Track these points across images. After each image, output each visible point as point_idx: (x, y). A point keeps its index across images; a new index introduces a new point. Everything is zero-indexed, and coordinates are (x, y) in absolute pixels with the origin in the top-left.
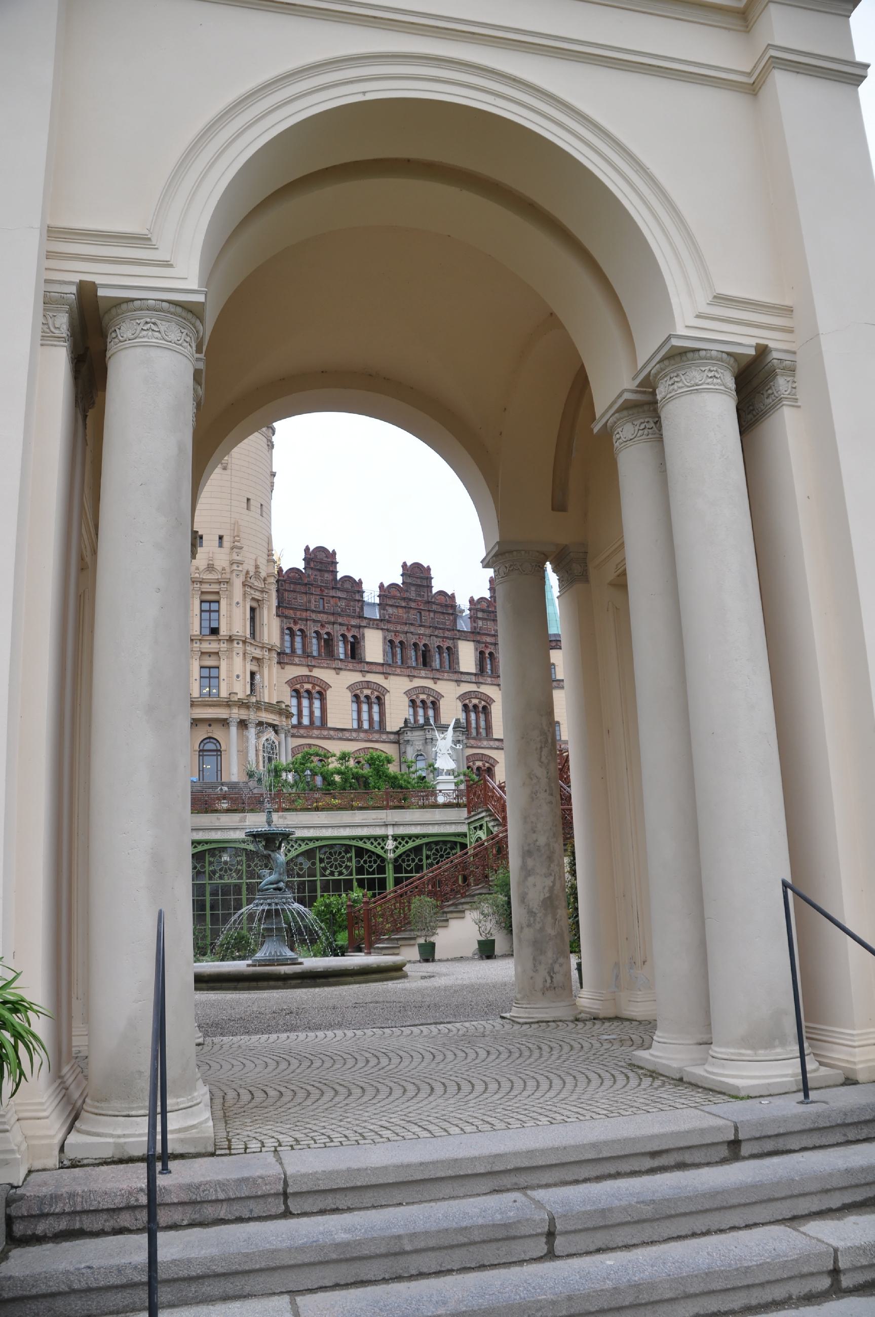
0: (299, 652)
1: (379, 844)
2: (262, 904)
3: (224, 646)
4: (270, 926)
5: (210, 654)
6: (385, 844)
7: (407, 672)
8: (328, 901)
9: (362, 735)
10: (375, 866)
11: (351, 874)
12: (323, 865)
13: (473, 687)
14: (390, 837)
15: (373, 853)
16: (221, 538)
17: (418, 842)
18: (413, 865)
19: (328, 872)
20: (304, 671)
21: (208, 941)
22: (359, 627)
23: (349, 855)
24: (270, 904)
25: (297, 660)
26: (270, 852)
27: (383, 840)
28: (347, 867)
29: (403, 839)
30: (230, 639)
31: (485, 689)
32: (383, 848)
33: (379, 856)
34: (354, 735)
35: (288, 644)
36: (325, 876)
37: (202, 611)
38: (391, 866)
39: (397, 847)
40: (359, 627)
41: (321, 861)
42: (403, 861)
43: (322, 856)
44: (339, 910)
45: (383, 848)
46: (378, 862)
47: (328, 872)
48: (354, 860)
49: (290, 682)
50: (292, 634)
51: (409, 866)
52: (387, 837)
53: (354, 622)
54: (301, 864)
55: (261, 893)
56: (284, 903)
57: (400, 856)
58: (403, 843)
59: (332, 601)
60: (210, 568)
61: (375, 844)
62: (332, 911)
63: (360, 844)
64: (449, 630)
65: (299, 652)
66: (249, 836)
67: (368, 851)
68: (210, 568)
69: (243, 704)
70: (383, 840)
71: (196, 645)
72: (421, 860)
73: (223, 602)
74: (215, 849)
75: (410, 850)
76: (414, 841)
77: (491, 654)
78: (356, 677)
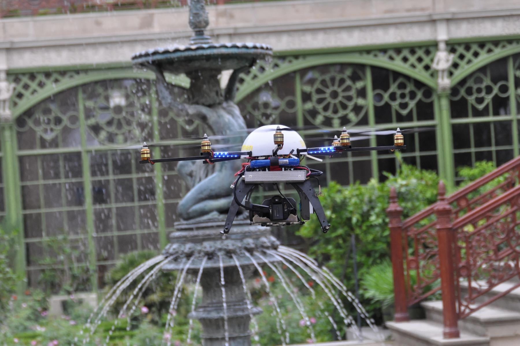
1: (420, 60)
2: (189, 256)
4: (214, 315)
6: (432, 60)
8: (338, 198)
10: (412, 104)
11: (364, 122)
12: (309, 106)
14: (442, 46)
15: (408, 78)
17: (498, 53)
18: (488, 99)
19: (320, 119)
21: (92, 265)
23: (359, 85)
24: (210, 256)
26: (205, 110)
27: (428, 53)
28: (357, 109)
29: (468, 48)
32: (427, 68)
33: (419, 84)
36: (315, 127)
38: (445, 103)
39: (455, 65)
41: (306, 97)
42: (469, 91)
43: (308, 89)
44: (365, 216)
45: (427, 68)
46: (419, 95)
47: (320, 119)
48: (370, 93)
51: (480, 101)
52: (435, 45)
54: (266, 105)
55: (183, 224)
56: (250, 251)
57: (463, 82)
58: (469, 55)
61: (413, 59)
62: (350, 219)
63: (382, 61)
66: (142, 65)
67: (397, 75)
70: (428, 53)
72: (504, 89)
74: (96, 83)
75: (483, 70)
76: (490, 51)
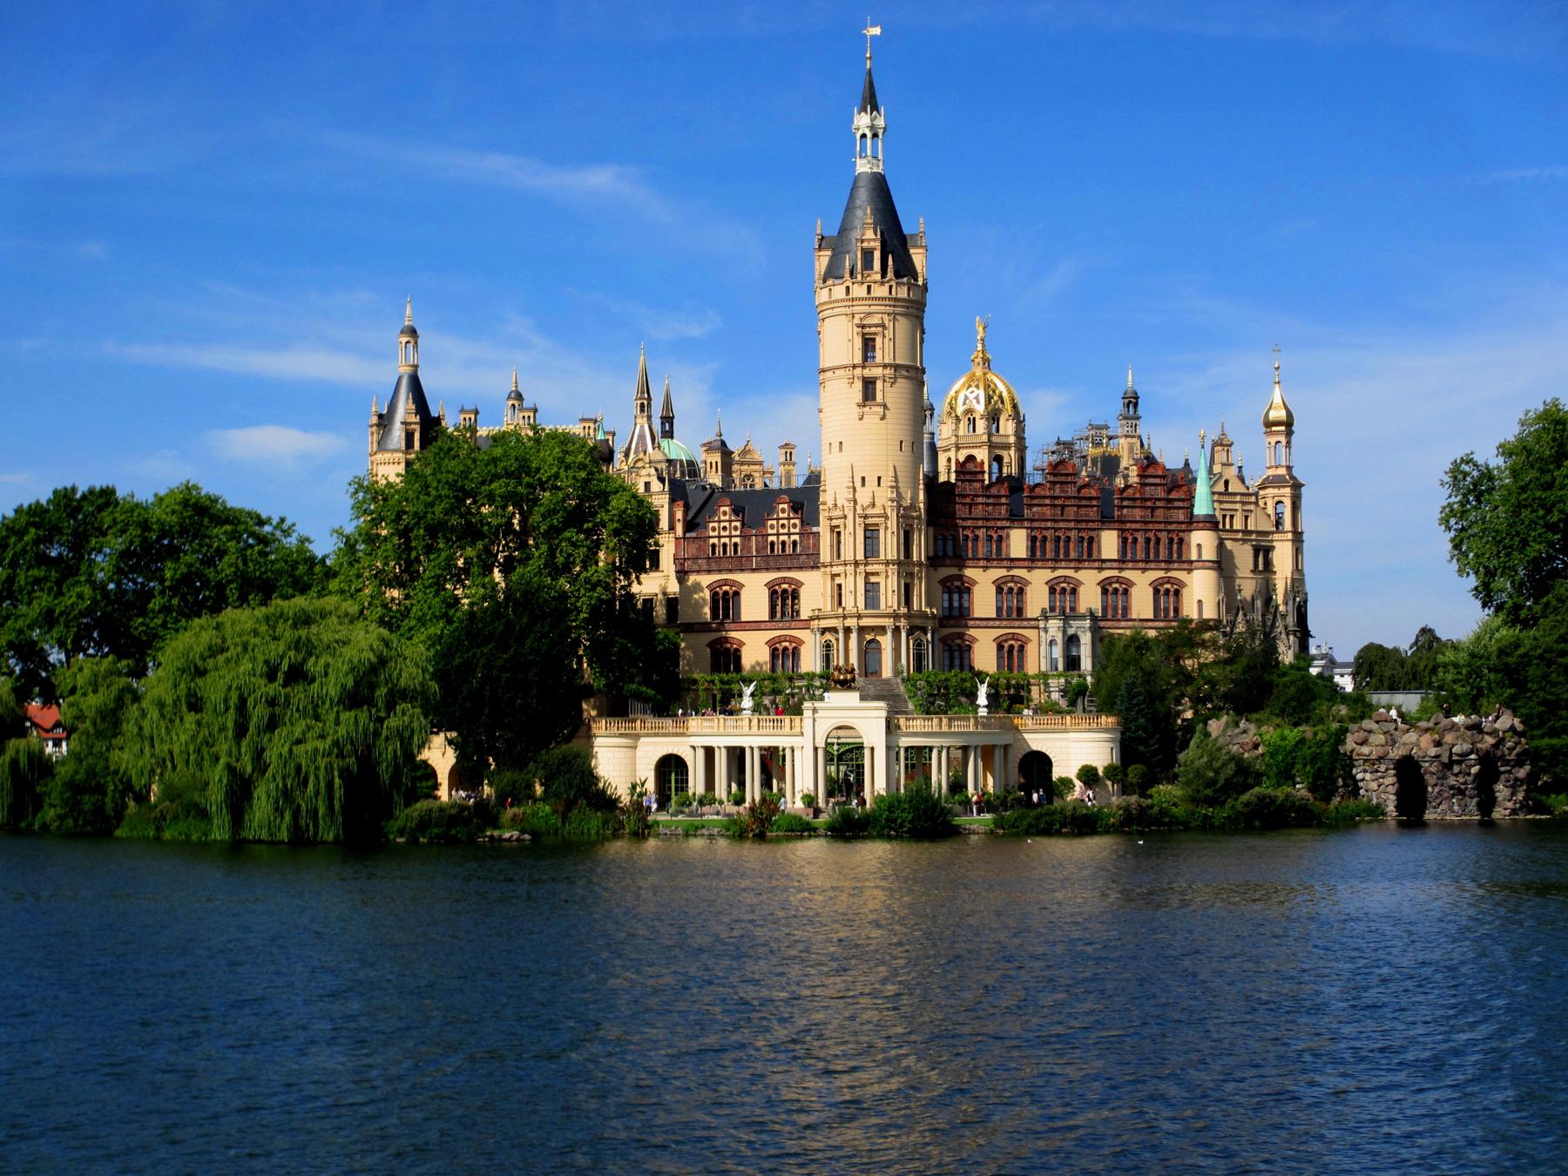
0: (950, 553)
3: (881, 568)
5: (873, 574)
7: (1050, 564)
9: (1004, 623)
13: (1115, 573)
16: (879, 478)
20: (954, 571)
22: (1002, 528)
25: (948, 562)
30: (887, 563)
31: (1125, 574)
34: (998, 623)
35: (941, 548)
37: (866, 538)
40: (1002, 528)
49: (943, 582)
50: (945, 540)
53: (999, 524)
59: (980, 507)
60: (873, 505)
64: (1093, 521)
65: (950, 553)
68: (873, 505)
69: (896, 616)
71: (861, 568)
73: (882, 532)
77: (1135, 540)
78: (1003, 572)
